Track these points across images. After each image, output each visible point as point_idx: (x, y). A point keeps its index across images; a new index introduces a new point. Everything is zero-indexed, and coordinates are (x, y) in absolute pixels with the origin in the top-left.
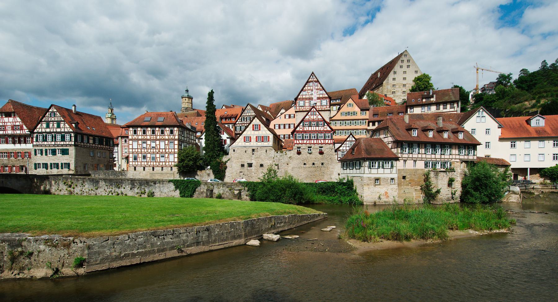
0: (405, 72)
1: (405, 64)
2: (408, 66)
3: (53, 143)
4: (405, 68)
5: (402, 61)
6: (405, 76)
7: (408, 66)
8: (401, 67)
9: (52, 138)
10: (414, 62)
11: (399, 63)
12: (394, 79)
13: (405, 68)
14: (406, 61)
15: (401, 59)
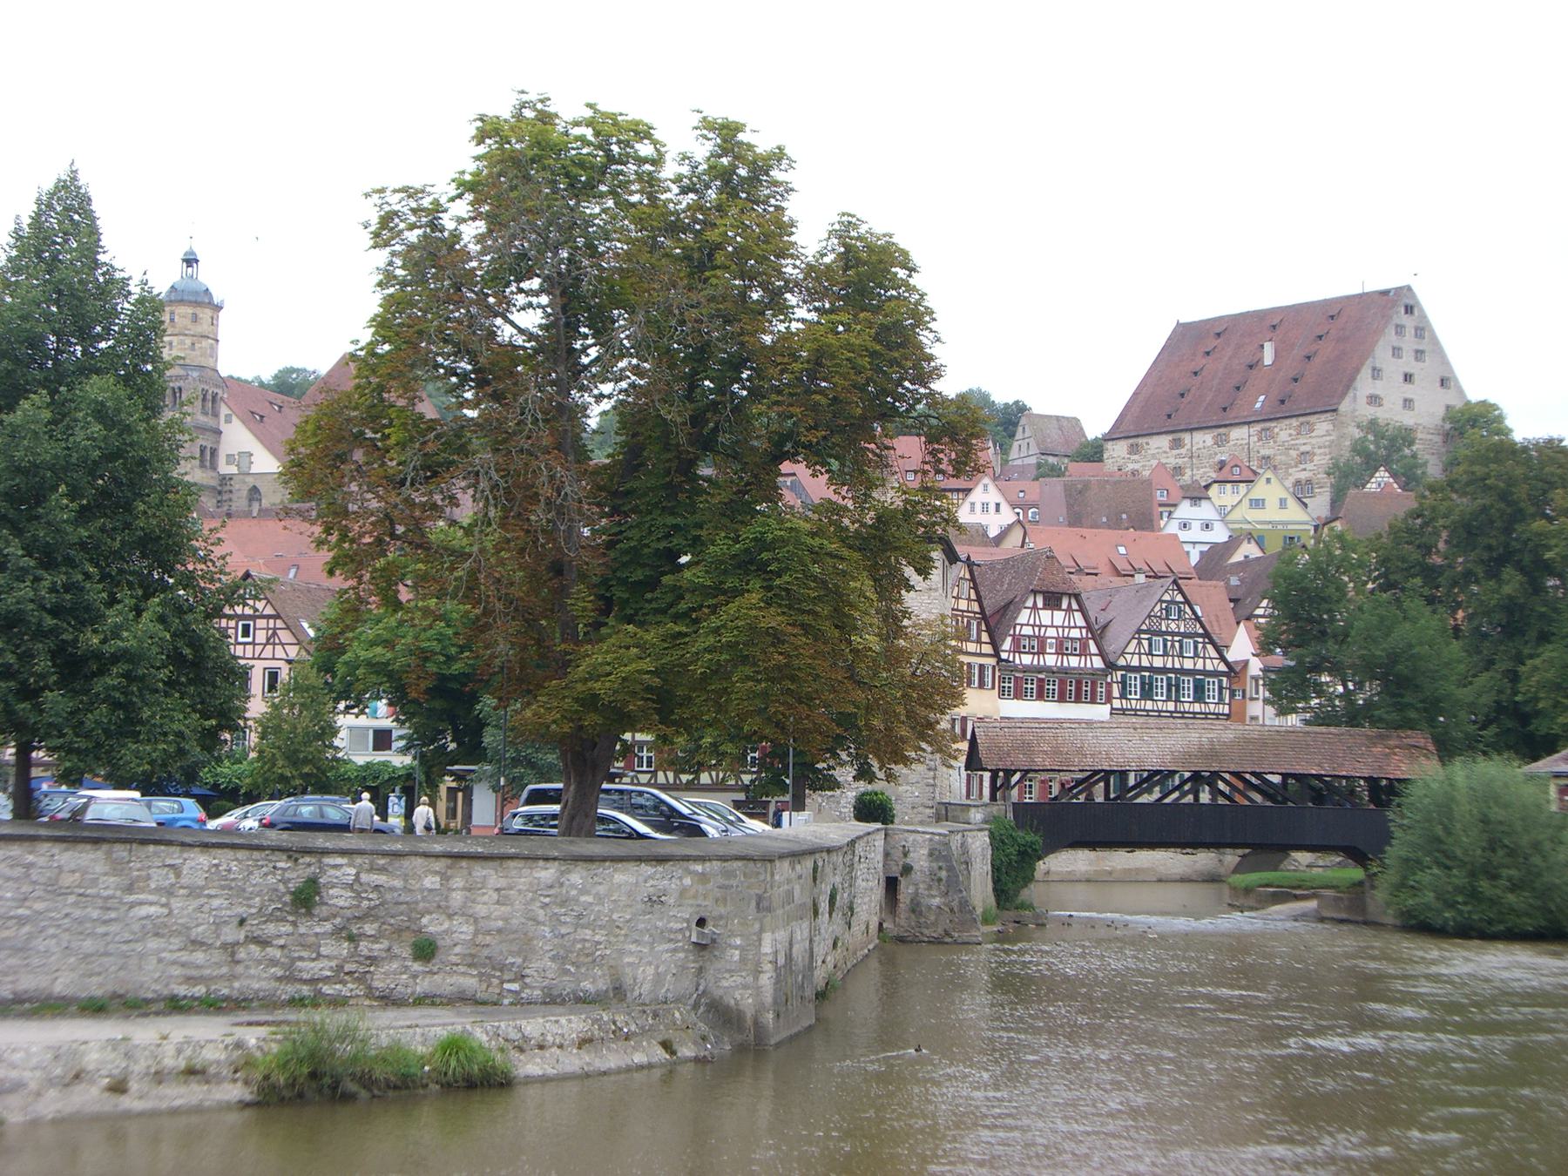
0: (1408, 378)
1: (1409, 343)
2: (1419, 354)
3: (1171, 706)
4: (1408, 363)
5: (1400, 329)
6: (1409, 391)
7: (1419, 354)
8: (1397, 352)
9: (1169, 690)
10: (1435, 341)
11: (1390, 336)
12: (1374, 400)
13: (1408, 363)
14: (1410, 332)
15: (1396, 320)
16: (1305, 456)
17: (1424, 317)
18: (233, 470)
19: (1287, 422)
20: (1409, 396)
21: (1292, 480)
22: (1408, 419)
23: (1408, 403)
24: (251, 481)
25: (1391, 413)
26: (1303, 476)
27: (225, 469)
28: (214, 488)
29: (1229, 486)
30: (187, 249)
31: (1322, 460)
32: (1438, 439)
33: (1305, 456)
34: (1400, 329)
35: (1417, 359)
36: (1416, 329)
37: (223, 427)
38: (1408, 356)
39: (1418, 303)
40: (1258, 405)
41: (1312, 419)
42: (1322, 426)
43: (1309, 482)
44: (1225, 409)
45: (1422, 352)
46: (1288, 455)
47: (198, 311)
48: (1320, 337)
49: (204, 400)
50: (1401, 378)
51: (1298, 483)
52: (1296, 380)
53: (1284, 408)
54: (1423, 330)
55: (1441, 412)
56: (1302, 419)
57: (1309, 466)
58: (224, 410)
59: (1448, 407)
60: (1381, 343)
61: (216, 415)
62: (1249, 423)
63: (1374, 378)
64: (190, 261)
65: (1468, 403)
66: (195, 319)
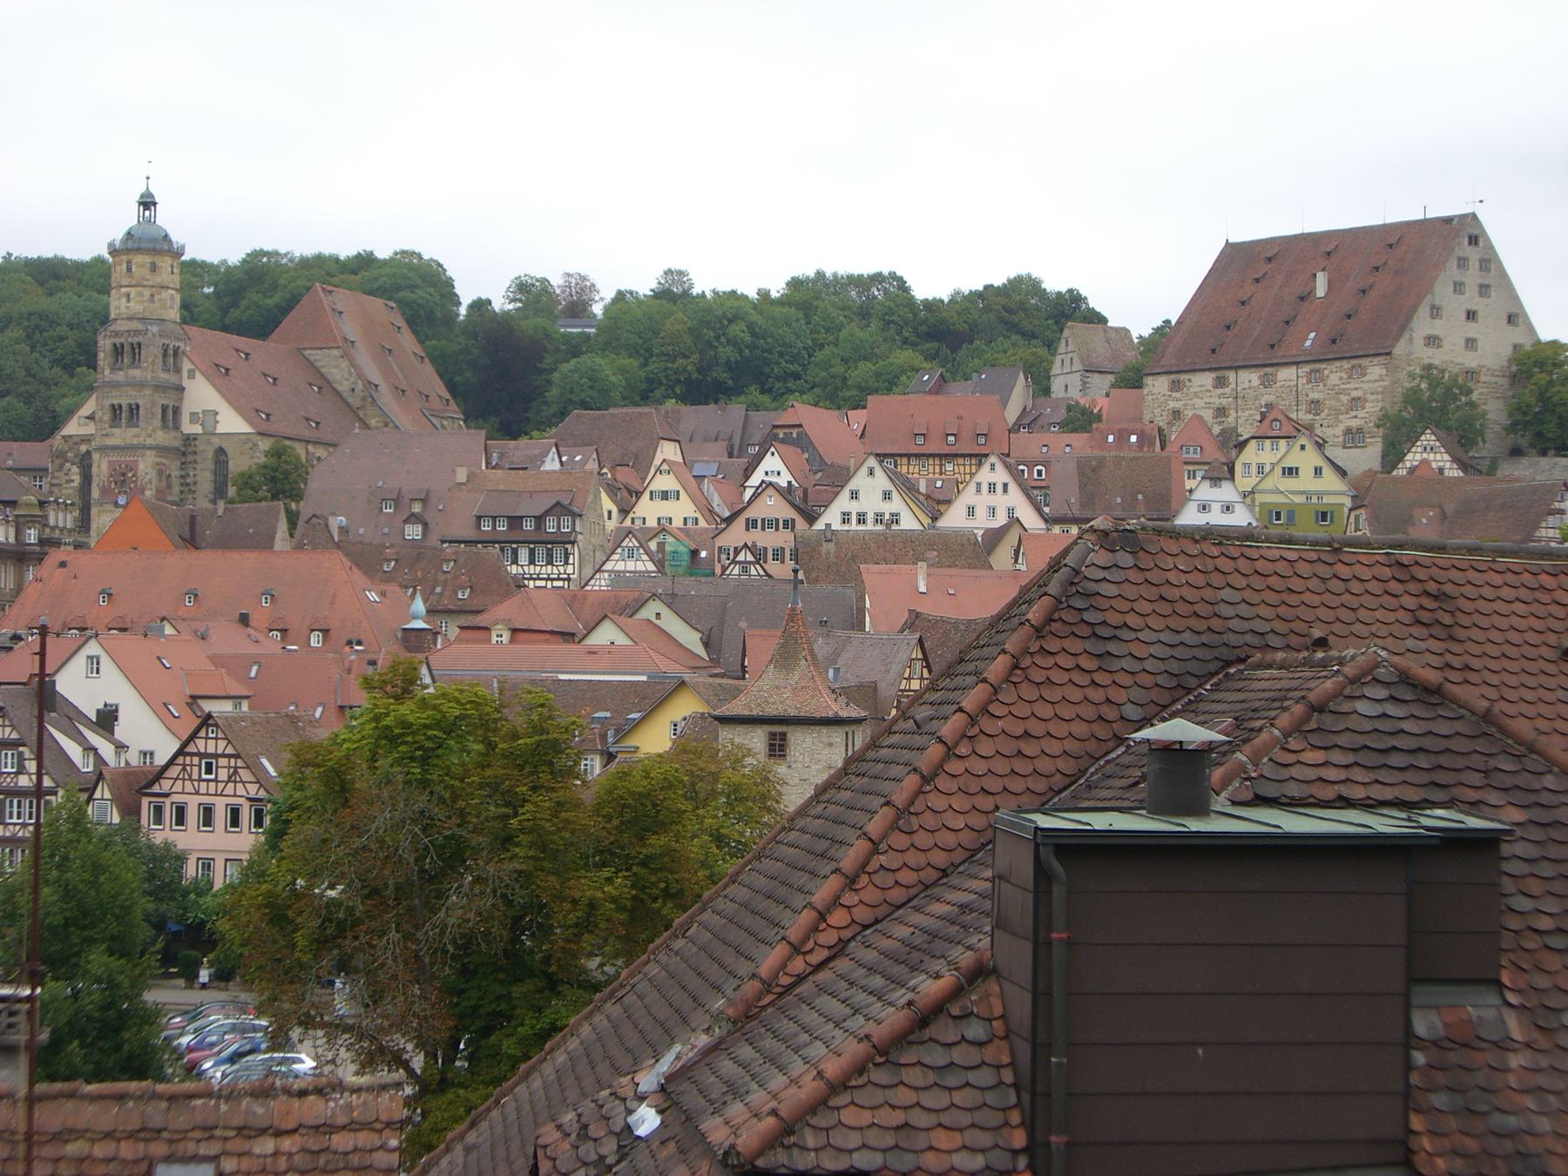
1: (1472, 277)
2: (1484, 289)
5: (1463, 263)
6: (1472, 330)
7: (1484, 289)
8: (1459, 287)
11: (1452, 271)
12: (1432, 341)
13: (1471, 299)
15: (1459, 253)
16: (1356, 403)
17: (1491, 247)
18: (198, 429)
19: (1338, 364)
20: (1471, 335)
21: (1342, 427)
22: (1470, 361)
23: (1470, 343)
24: (216, 441)
25: (1452, 356)
26: (1354, 423)
27: (189, 428)
28: (177, 449)
29: (1268, 442)
30: (143, 189)
31: (1373, 408)
32: (1504, 382)
33: (1356, 403)
34: (1463, 263)
35: (1481, 295)
36: (1481, 261)
37: (186, 383)
38: (1471, 291)
39: (1484, 232)
40: (1308, 343)
41: (1365, 362)
42: (1375, 370)
43: (1360, 430)
44: (1272, 346)
45: (1488, 286)
46: (1338, 400)
47: (159, 261)
48: (1377, 269)
49: (165, 355)
50: (1464, 316)
51: (1348, 431)
52: (1349, 317)
53: (1335, 349)
54: (1490, 261)
55: (1507, 351)
56: (1354, 362)
57: (1361, 414)
58: (187, 366)
59: (1515, 346)
60: (1442, 277)
61: (178, 370)
62: (1297, 363)
63: (1432, 317)
64: (147, 203)
65: (1538, 342)
66: (154, 268)
